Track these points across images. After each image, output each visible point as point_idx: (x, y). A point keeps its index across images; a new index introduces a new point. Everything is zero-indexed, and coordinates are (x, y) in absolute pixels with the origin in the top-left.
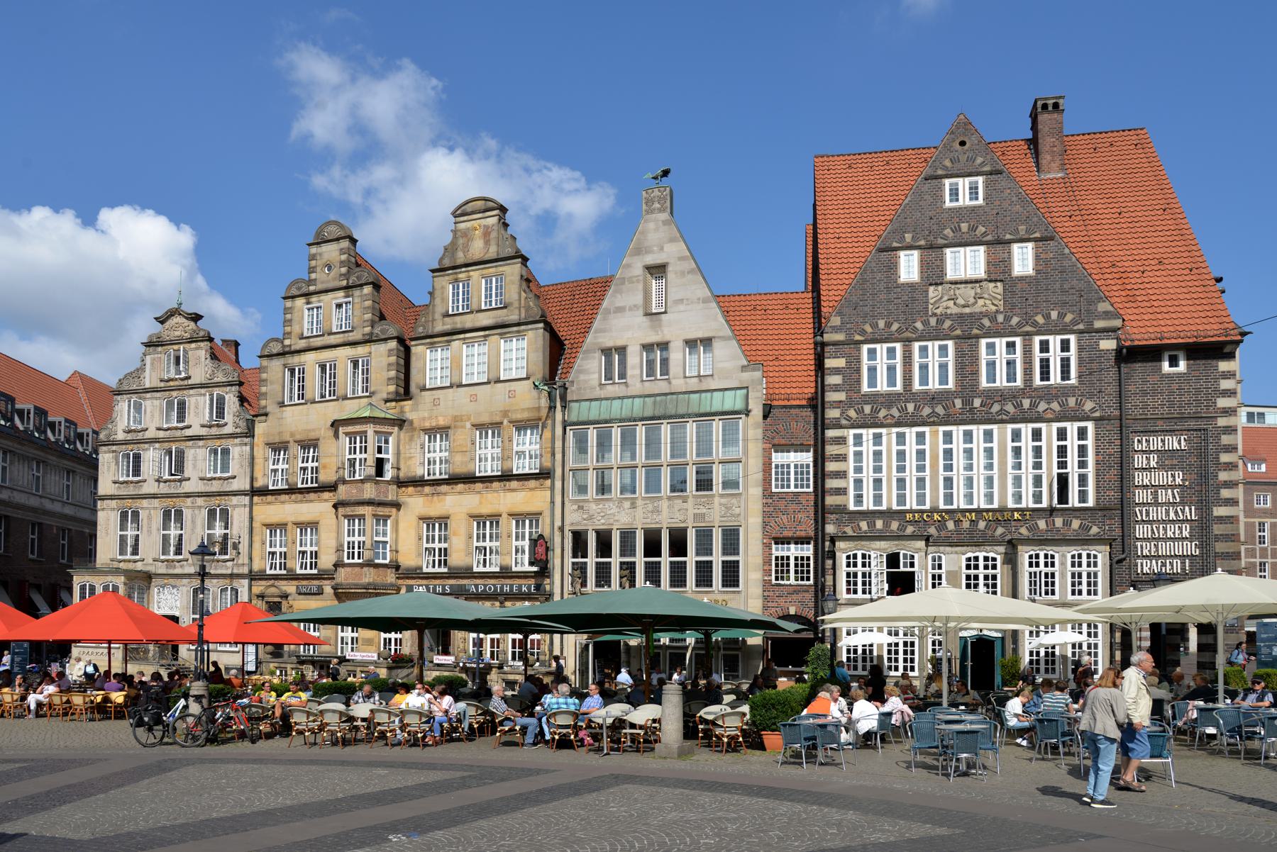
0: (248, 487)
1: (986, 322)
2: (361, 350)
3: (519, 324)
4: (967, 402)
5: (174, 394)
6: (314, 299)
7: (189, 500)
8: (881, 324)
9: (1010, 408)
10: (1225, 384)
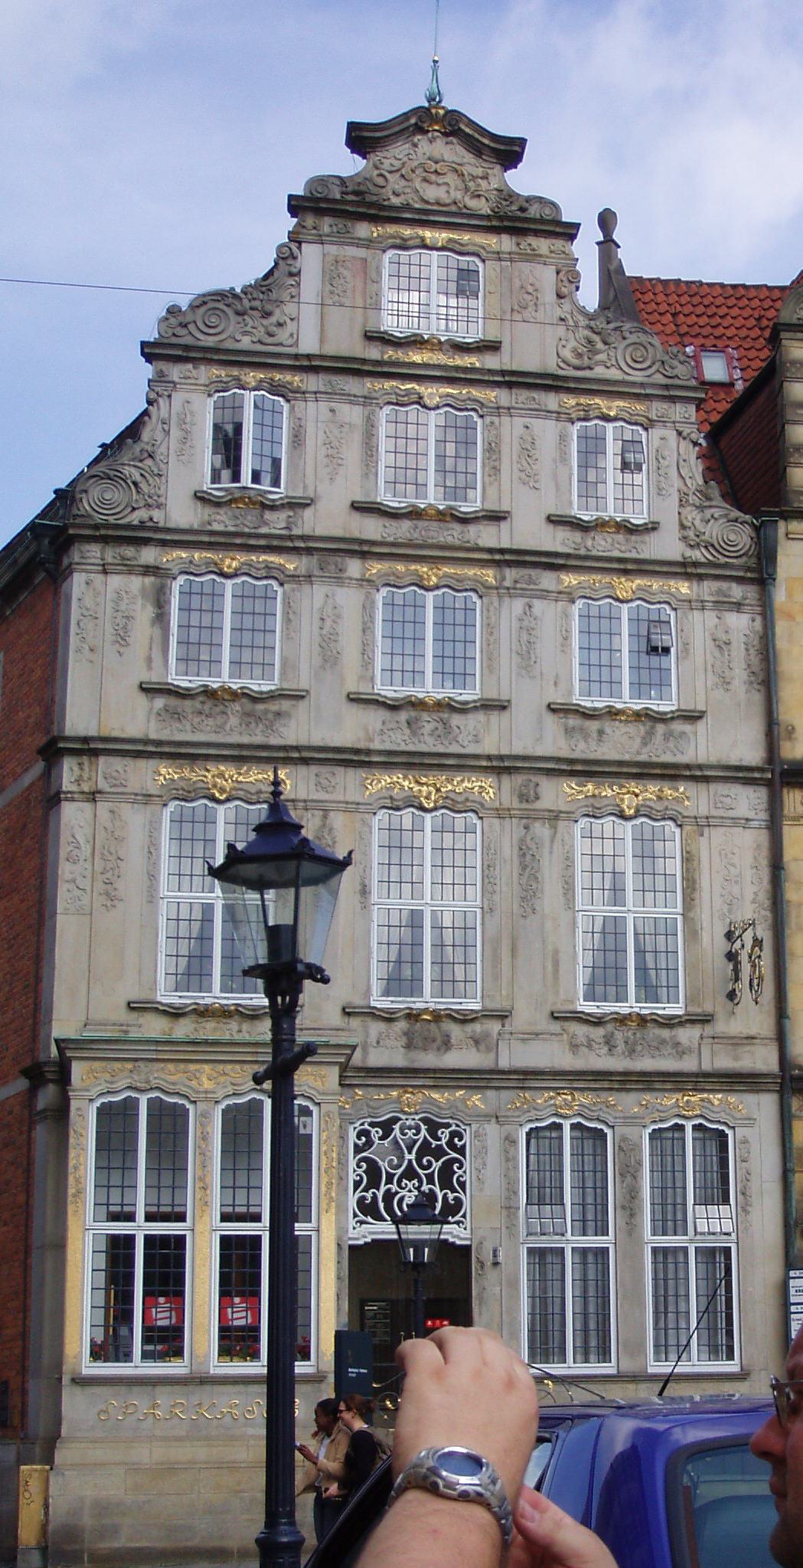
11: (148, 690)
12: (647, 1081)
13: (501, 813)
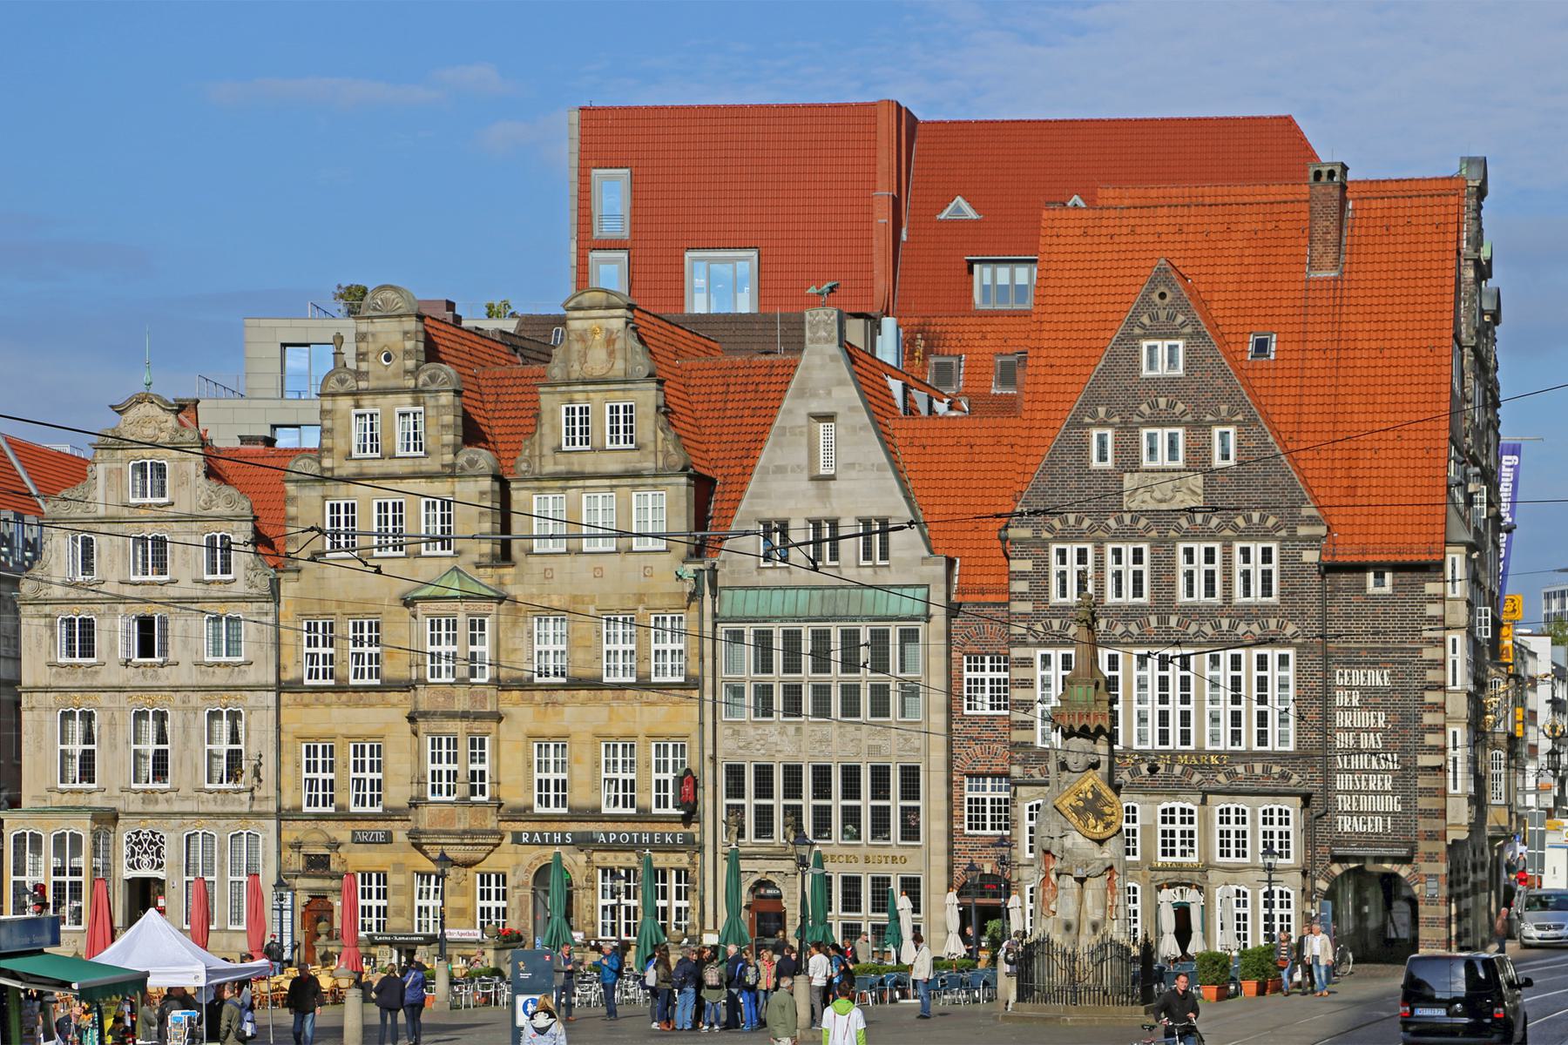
0: (272, 679)
1: (1184, 522)
2: (441, 488)
3: (655, 476)
4: (1163, 620)
6: (366, 401)
9: (1207, 629)
11: (51, 665)
12: (227, 815)
13: (176, 709)
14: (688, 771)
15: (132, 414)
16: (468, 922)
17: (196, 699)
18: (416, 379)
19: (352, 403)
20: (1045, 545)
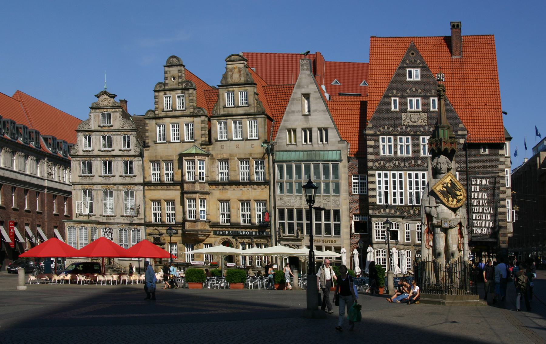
0: (142, 181)
2: (189, 120)
4: (416, 162)
5: (106, 134)
6: (168, 93)
7: (115, 187)
8: (386, 127)
10: (502, 159)
11: (80, 176)
13: (115, 190)
14: (267, 211)
15: (101, 97)
16: (201, 259)
17: (121, 187)
18: (182, 85)
19: (163, 93)
20: (378, 136)
